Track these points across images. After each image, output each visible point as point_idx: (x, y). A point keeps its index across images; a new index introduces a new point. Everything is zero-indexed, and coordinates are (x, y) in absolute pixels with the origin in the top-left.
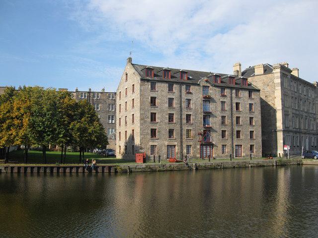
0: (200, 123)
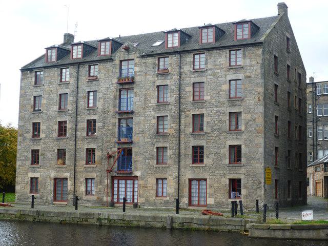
0: (113, 135)
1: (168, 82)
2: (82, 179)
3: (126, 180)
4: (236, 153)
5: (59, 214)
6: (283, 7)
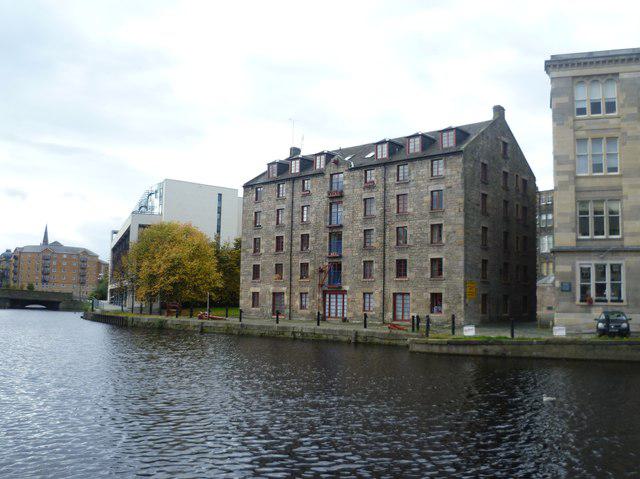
0: (324, 250)
1: (373, 195)
2: (297, 294)
3: (336, 294)
4: (437, 263)
5: (260, 327)
6: (499, 111)
